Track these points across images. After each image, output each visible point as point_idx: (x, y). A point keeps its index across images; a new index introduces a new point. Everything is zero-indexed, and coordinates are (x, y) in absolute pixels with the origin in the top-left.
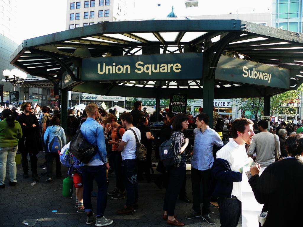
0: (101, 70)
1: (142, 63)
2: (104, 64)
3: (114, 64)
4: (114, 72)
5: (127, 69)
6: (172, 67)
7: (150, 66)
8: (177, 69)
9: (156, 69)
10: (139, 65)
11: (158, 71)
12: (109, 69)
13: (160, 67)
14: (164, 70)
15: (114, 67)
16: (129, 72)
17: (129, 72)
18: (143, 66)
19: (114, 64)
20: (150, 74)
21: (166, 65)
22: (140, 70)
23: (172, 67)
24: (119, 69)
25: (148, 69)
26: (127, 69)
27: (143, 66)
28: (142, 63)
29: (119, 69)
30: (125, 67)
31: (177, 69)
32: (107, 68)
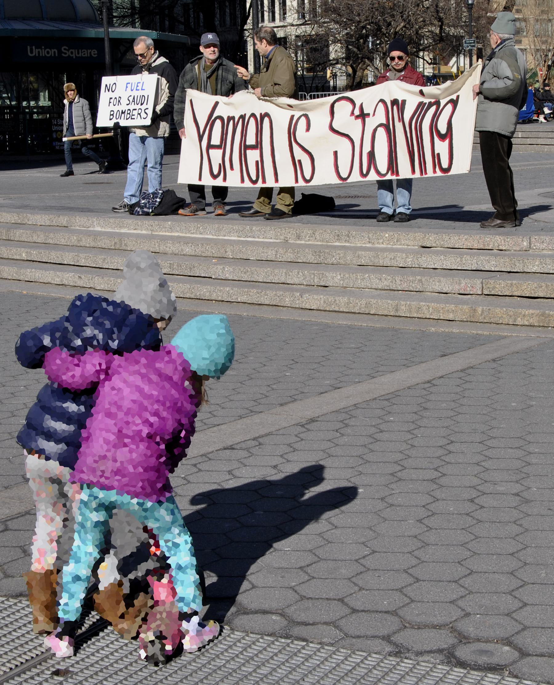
0: (32, 52)
1: (67, 48)
2: (34, 47)
3: (43, 47)
4: (44, 55)
5: (55, 52)
6: (90, 53)
7: (73, 51)
8: (94, 54)
9: (78, 53)
10: (65, 49)
11: (80, 55)
12: (39, 52)
13: (82, 52)
14: (84, 54)
15: (43, 50)
16: (57, 55)
17: (57, 55)
18: (68, 50)
19: (43, 47)
20: (74, 57)
21: (85, 50)
22: (66, 54)
23: (90, 53)
24: (48, 53)
25: (72, 53)
26: (55, 52)
27: (68, 50)
28: (67, 48)
29: (48, 53)
30: (53, 50)
31: (94, 54)
32: (37, 50)
